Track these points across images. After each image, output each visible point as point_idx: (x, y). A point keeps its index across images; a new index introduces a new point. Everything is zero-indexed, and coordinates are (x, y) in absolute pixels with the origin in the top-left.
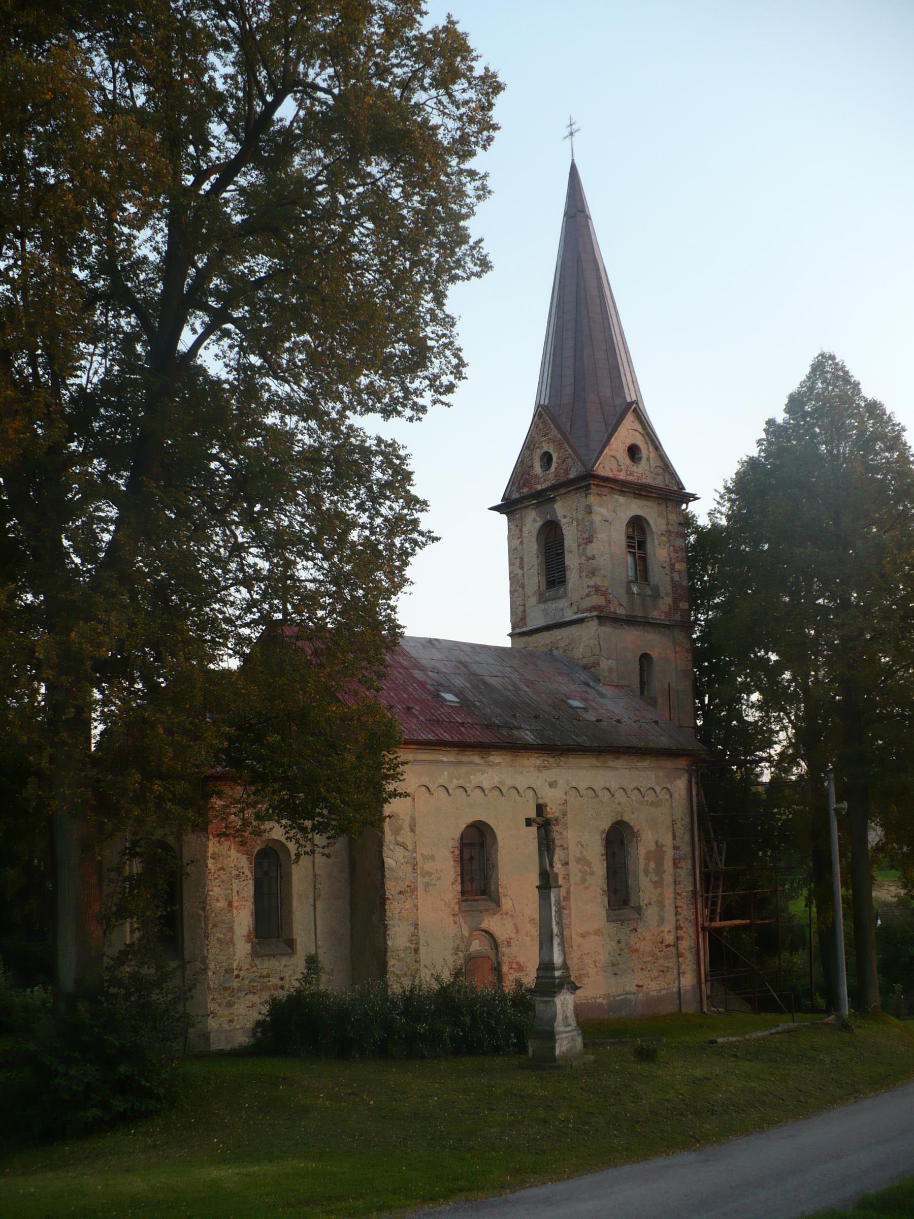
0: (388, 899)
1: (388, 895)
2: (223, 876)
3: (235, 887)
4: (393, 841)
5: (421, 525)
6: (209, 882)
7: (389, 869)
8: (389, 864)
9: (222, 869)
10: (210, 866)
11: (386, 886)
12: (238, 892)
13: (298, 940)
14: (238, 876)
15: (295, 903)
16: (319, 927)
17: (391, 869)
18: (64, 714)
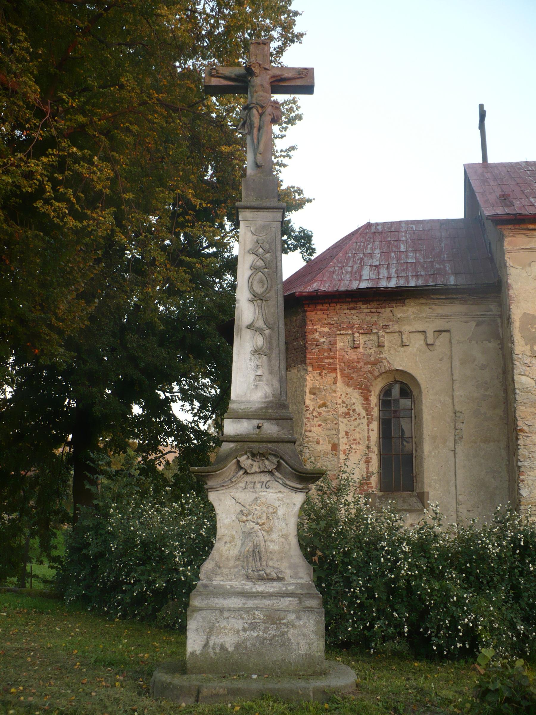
0: (521, 430)
1: (521, 424)
2: (324, 414)
3: (342, 427)
4: (529, 353)
5: (279, 101)
6: (306, 421)
7: (522, 390)
8: (521, 384)
9: (324, 405)
10: (308, 402)
11: (518, 413)
12: (347, 433)
13: (431, 494)
14: (347, 414)
15: (427, 447)
16: (460, 476)
17: (527, 391)
18: (196, 206)
